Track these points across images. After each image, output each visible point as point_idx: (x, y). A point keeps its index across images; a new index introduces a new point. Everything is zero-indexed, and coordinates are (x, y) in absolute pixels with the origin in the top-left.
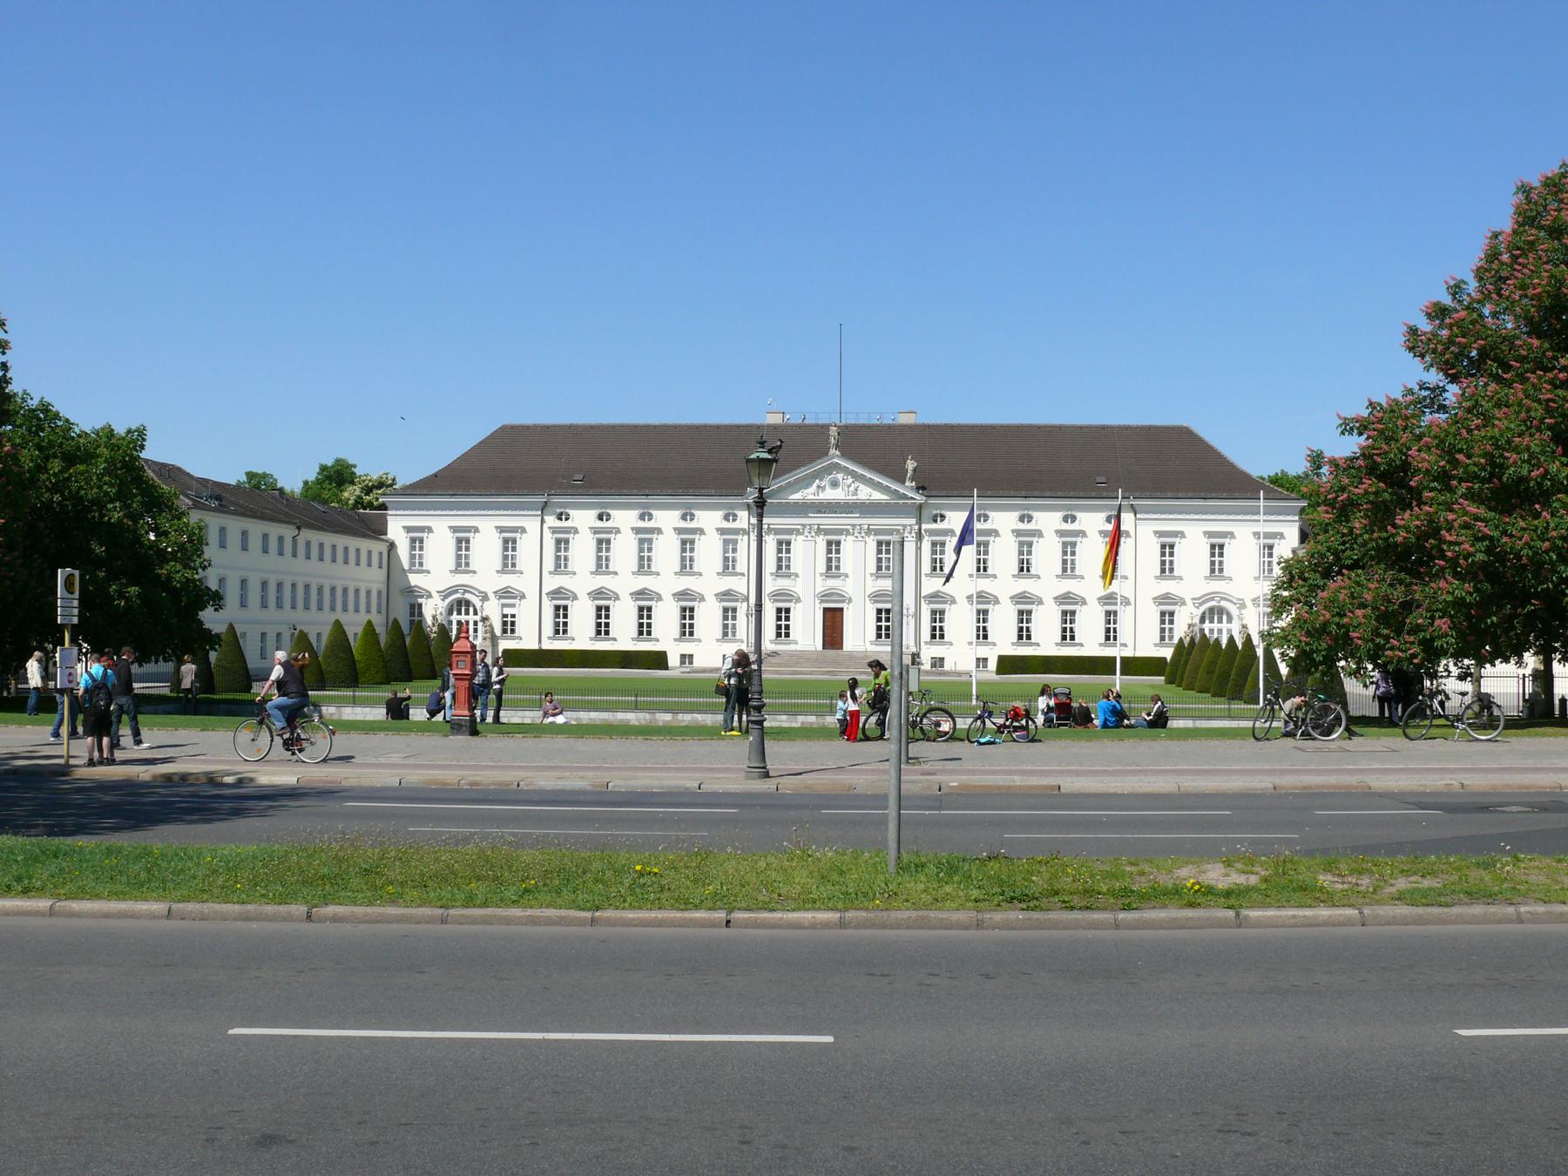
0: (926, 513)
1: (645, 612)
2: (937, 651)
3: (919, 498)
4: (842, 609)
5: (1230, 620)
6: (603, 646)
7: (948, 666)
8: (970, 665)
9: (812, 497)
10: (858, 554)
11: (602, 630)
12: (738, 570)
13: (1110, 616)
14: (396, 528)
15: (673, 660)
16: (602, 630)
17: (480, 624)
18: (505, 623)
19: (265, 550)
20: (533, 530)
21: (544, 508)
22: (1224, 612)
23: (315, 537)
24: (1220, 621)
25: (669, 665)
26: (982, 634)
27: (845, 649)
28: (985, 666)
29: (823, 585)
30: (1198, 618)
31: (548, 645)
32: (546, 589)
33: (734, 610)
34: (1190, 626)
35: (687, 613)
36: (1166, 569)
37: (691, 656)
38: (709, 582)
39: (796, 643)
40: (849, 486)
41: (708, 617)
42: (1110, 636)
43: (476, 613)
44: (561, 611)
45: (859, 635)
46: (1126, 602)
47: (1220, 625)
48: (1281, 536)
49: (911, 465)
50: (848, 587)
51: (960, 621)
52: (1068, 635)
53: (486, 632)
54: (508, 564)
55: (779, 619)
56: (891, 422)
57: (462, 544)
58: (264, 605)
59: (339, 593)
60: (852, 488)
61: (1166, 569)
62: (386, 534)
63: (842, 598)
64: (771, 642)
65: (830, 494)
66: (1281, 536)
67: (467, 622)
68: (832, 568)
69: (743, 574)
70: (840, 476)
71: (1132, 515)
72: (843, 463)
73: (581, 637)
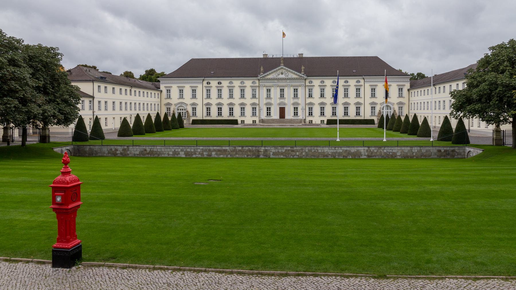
0: (307, 81)
1: (231, 109)
2: (310, 118)
3: (305, 77)
4: (285, 107)
5: (390, 109)
6: (220, 118)
7: (314, 122)
8: (319, 122)
9: (276, 77)
10: (289, 92)
11: (220, 114)
12: (256, 97)
13: (358, 108)
14: (162, 87)
15: (239, 122)
16: (220, 114)
17: (186, 113)
18: (193, 113)
19: (121, 93)
20: (200, 87)
21: (203, 80)
22: (389, 108)
23: (137, 90)
24: (388, 109)
25: (239, 123)
26: (322, 114)
27: (285, 118)
28: (324, 122)
29: (278, 101)
30: (382, 108)
31: (204, 118)
33: (255, 108)
34: (380, 111)
35: (243, 109)
36: (373, 95)
37: (244, 121)
38: (248, 100)
39: (272, 116)
40: (286, 74)
41: (248, 110)
42: (358, 114)
44: (208, 109)
45: (289, 115)
46: (362, 104)
47: (388, 111)
49: (303, 68)
50: (286, 101)
51: (316, 111)
52: (346, 114)
53: (188, 115)
54: (194, 96)
55: (268, 110)
56: (296, 57)
57: (181, 91)
58: (121, 109)
59: (146, 105)
60: (287, 74)
61: (373, 95)
62: (160, 89)
63: (285, 104)
64: (265, 116)
65: (281, 76)
66: (405, 85)
67: (183, 113)
68: (282, 96)
70: (284, 71)
71: (363, 80)
72: (284, 68)
73: (214, 115)
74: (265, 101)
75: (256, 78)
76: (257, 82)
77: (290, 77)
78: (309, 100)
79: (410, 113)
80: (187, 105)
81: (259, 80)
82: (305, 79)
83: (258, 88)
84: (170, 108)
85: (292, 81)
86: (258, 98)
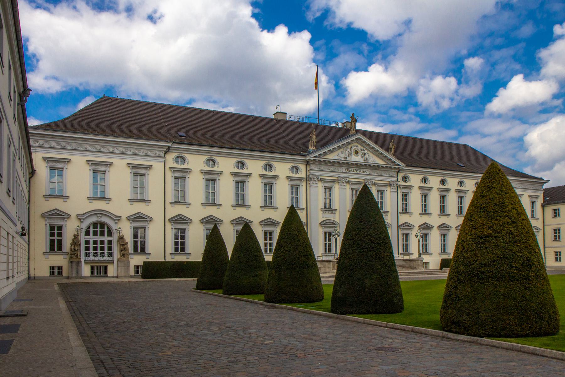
0: (401, 175)
3: (402, 165)
18: (136, 243)
31: (169, 259)
32: (168, 216)
43: (110, 234)
48: (537, 197)
60: (367, 156)
67: (102, 242)
69: (303, 209)
74: (321, 217)
75: (303, 158)
76: (302, 167)
77: (370, 161)
78: (404, 219)
79: (546, 246)
80: (117, 219)
81: (308, 163)
82: (399, 171)
83: (304, 184)
84: (60, 228)
85: (375, 172)
86: (304, 206)
